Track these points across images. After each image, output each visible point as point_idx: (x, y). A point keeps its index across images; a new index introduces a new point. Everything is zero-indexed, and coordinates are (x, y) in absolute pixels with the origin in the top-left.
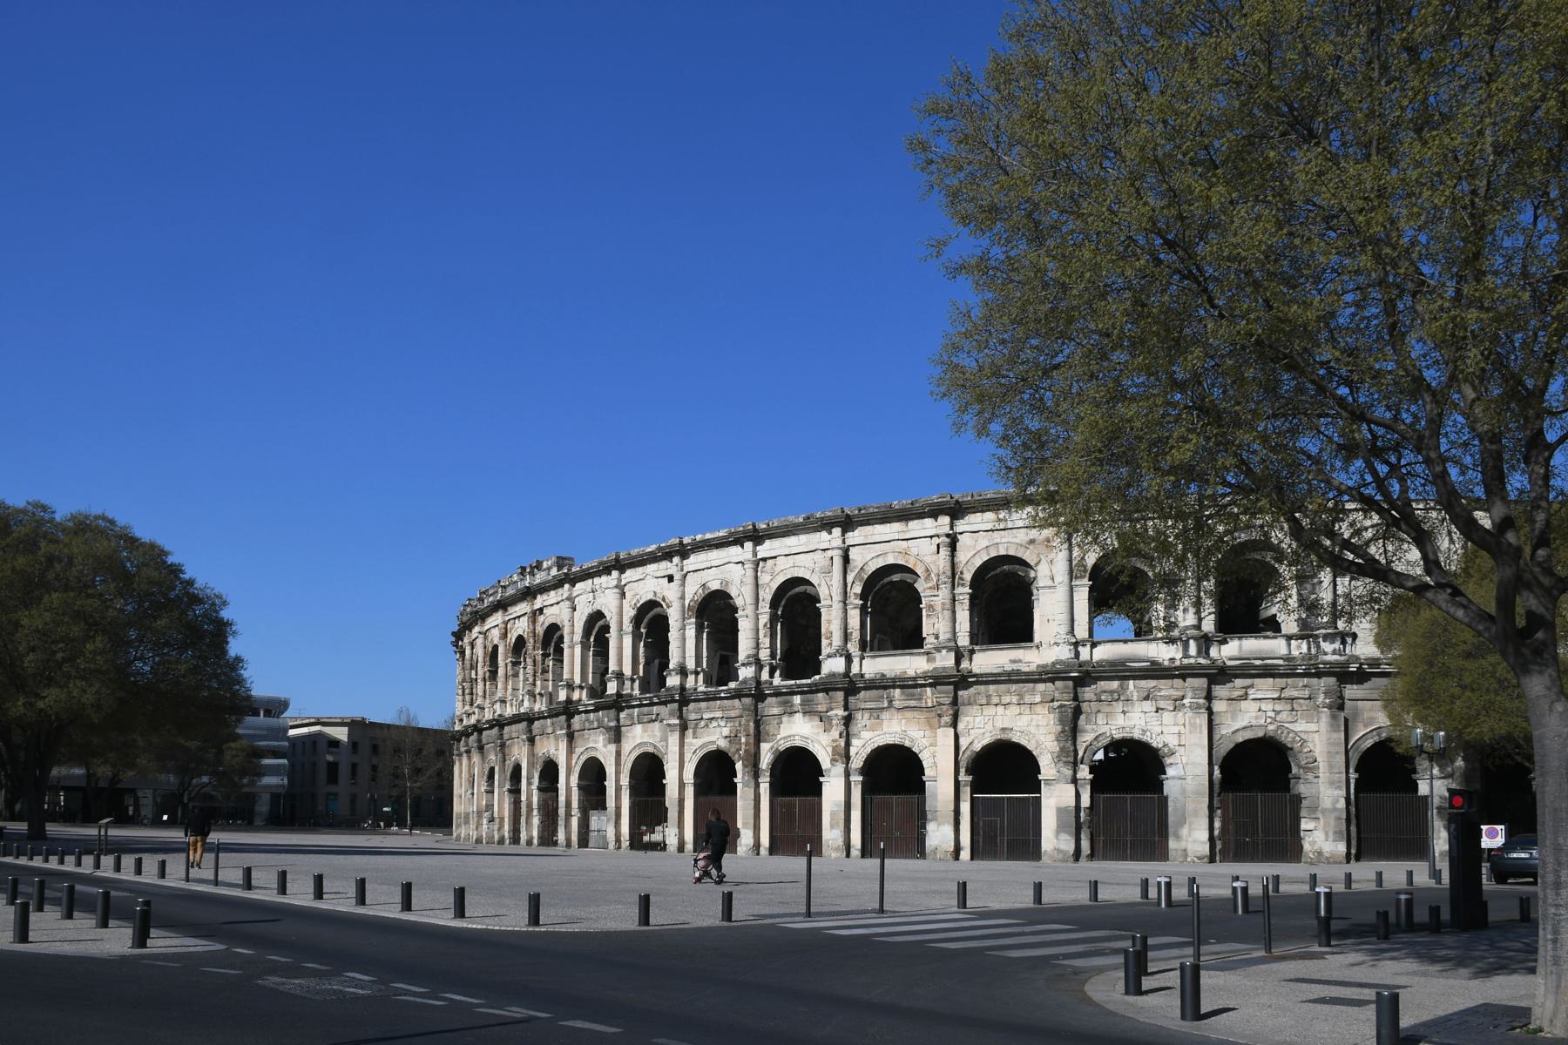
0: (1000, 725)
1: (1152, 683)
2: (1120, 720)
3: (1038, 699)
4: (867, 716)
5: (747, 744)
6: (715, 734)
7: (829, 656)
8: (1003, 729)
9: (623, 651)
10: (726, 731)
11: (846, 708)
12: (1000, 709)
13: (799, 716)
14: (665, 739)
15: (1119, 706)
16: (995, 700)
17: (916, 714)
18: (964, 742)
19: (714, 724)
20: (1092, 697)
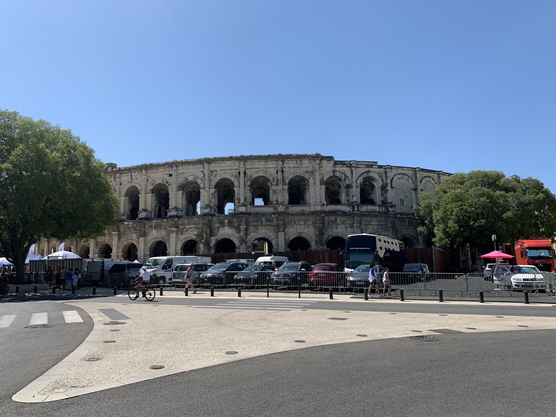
0: (298, 231)
3: (311, 223)
4: (253, 227)
6: (191, 234)
7: (240, 206)
8: (300, 233)
9: (147, 202)
10: (195, 233)
12: (298, 226)
13: (226, 228)
14: (168, 235)
16: (297, 223)
17: (270, 227)
18: (287, 237)
19: (191, 230)
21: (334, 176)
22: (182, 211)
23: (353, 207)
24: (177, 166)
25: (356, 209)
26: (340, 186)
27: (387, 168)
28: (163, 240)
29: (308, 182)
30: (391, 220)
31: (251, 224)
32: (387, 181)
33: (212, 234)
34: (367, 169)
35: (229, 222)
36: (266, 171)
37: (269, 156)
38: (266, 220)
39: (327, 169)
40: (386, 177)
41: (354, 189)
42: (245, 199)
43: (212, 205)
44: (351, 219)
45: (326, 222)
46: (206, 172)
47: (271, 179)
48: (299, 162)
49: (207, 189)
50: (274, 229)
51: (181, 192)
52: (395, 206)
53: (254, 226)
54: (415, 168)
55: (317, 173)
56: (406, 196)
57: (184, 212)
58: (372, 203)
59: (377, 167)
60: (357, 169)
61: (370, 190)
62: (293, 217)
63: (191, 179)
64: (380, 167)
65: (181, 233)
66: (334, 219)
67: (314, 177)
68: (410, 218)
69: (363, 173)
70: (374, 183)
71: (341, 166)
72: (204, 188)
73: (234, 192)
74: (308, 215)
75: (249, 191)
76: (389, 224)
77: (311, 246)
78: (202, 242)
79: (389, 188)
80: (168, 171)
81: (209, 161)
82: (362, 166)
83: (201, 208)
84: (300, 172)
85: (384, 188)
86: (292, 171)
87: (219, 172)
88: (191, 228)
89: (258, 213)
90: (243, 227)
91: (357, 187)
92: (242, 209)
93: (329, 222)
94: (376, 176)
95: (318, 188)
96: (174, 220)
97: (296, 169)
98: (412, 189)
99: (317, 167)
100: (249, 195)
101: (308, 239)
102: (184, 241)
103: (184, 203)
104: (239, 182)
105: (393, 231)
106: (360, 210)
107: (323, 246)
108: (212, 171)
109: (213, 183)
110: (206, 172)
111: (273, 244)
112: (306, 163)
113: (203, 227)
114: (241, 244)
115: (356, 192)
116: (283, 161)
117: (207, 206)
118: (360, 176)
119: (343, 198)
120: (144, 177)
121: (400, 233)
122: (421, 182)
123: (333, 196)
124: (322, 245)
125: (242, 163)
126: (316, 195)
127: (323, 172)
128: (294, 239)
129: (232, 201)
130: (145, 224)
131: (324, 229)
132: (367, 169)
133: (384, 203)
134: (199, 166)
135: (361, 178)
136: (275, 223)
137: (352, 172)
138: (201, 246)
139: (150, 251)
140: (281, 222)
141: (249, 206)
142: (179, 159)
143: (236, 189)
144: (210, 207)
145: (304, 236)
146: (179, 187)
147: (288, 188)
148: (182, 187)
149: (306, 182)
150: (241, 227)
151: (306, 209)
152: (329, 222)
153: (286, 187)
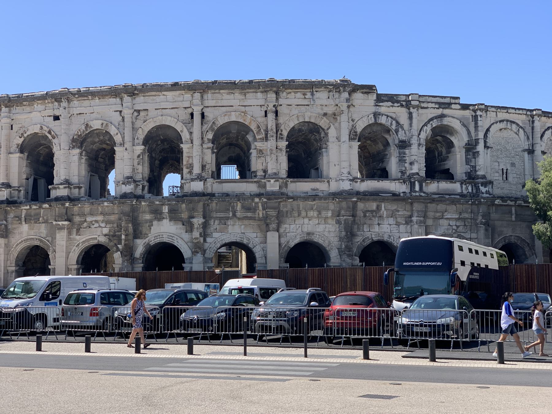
1: (395, 207)
2: (376, 229)
3: (330, 214)
4: (217, 222)
5: (125, 240)
6: (97, 233)
7: (192, 180)
8: (308, 234)
10: (106, 231)
11: (204, 217)
12: (306, 221)
13: (166, 222)
15: (376, 221)
16: (303, 214)
17: (251, 222)
18: (283, 240)
19: (96, 225)
20: (362, 215)
21: (376, 124)
22: (80, 188)
23: (412, 185)
24: (69, 101)
25: (417, 188)
26: (387, 144)
27: (476, 111)
28: (41, 245)
29: (326, 134)
30: (483, 209)
31: (214, 215)
32: (477, 135)
33: (137, 234)
34: (440, 111)
35: (171, 211)
36: (245, 113)
37: (251, 82)
38: (243, 207)
39: (363, 111)
40: (476, 127)
41: (414, 148)
42: (203, 167)
43: (139, 177)
44: (408, 207)
45: (360, 213)
46: (127, 113)
47: (253, 127)
48: (309, 95)
49: (128, 145)
50: (259, 226)
51: (77, 151)
52: (491, 182)
53: (220, 219)
54: (532, 111)
55: (344, 118)
56: (513, 165)
57: (83, 190)
58: (448, 176)
59: (458, 107)
60: (421, 111)
61: (444, 151)
62: (295, 203)
63: (96, 125)
64: (465, 107)
65: (78, 231)
66: (374, 208)
67: (337, 124)
68: (520, 206)
69: (432, 119)
70: (452, 139)
71: (390, 104)
72: (122, 144)
73: (181, 152)
74: (325, 199)
75: (210, 151)
76: (480, 218)
77: (329, 259)
78: (118, 249)
79: (480, 147)
80: (53, 108)
81: (132, 91)
82: (430, 105)
83: (117, 183)
84: (311, 115)
85: (471, 148)
86: (295, 111)
87: (152, 113)
88: (97, 221)
89: (228, 195)
90: (198, 221)
91: (419, 145)
92: (198, 186)
93: (365, 213)
94: (456, 124)
95: (345, 147)
96: (63, 205)
97: (303, 108)
98: (524, 150)
99: (344, 106)
100: (210, 158)
101: (325, 244)
102: (82, 247)
103: (83, 172)
104: (191, 133)
105: (486, 230)
106: (425, 189)
107: (352, 259)
108: (139, 111)
109: (141, 135)
110: (127, 113)
111: (257, 255)
112: (322, 96)
113: (120, 219)
114: (194, 253)
115: (417, 156)
116: (277, 93)
117: (129, 180)
118: (426, 125)
119: (393, 166)
120: (5, 121)
121: (499, 236)
122: (542, 136)
123: (373, 163)
124: (349, 256)
125: (197, 95)
126: (340, 160)
127: (356, 117)
128: (297, 245)
129: (178, 169)
130: (6, 213)
131: (356, 227)
132: (440, 111)
133: (471, 177)
134: (112, 100)
135: (428, 128)
136: (260, 213)
137: (411, 117)
138: (117, 256)
139: (17, 265)
140: (273, 213)
141: (210, 181)
142: (73, 88)
143: (184, 147)
144: (135, 181)
145: (316, 239)
146: (73, 140)
147: (288, 147)
148: (79, 142)
149: (322, 135)
150: (195, 221)
151: (321, 186)
152: (365, 213)
153: (283, 144)
